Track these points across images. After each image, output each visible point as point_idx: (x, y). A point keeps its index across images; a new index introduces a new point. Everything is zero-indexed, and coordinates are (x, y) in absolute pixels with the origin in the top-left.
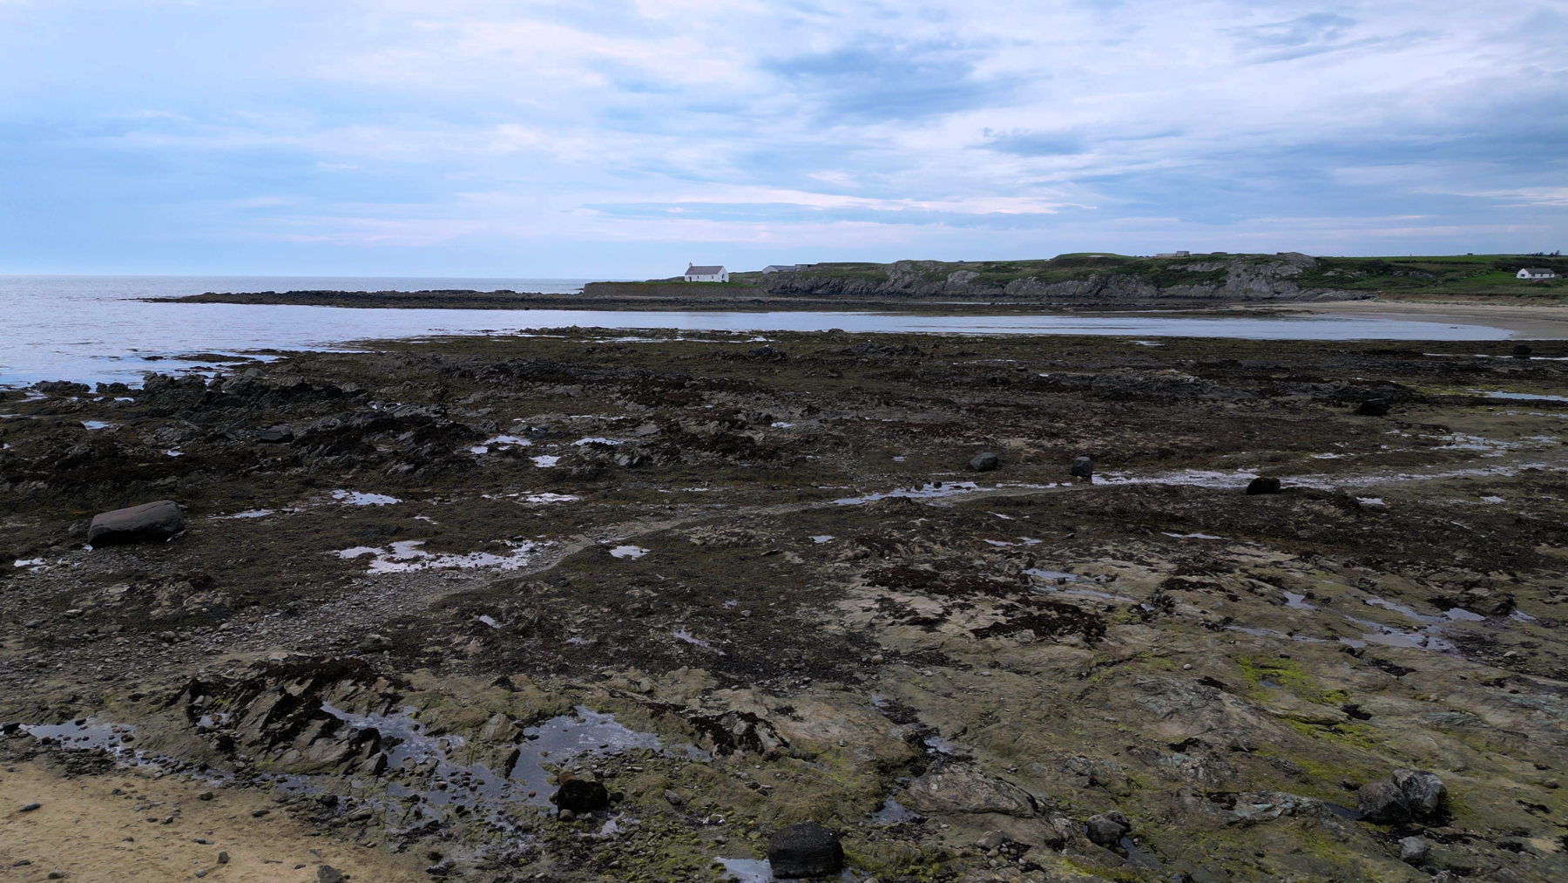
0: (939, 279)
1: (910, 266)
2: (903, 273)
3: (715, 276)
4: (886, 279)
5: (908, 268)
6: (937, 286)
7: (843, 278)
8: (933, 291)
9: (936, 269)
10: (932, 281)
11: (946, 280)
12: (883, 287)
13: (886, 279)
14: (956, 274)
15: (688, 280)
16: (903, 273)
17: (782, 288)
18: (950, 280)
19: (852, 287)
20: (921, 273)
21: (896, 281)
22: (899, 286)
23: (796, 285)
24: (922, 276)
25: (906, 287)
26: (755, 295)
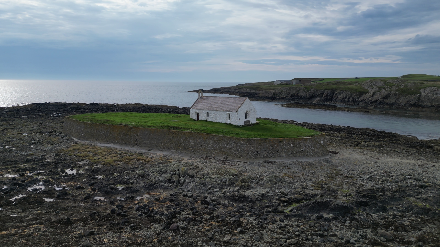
0: (414, 93)
1: (382, 83)
2: (379, 88)
3: (233, 115)
4: (366, 92)
5: (381, 84)
6: (413, 98)
7: (333, 91)
8: (412, 102)
9: (406, 86)
10: (407, 95)
11: (421, 94)
12: (364, 97)
13: (366, 92)
14: (428, 89)
15: (195, 117)
16: (379, 88)
17: (291, 96)
18: (424, 94)
19: (341, 96)
20: (394, 89)
21: (374, 93)
22: (377, 97)
23: (301, 94)
24: (397, 90)
25: (385, 97)
26: (304, 154)
